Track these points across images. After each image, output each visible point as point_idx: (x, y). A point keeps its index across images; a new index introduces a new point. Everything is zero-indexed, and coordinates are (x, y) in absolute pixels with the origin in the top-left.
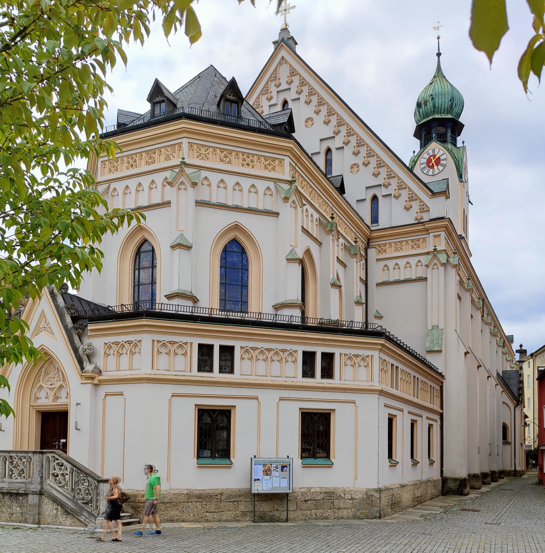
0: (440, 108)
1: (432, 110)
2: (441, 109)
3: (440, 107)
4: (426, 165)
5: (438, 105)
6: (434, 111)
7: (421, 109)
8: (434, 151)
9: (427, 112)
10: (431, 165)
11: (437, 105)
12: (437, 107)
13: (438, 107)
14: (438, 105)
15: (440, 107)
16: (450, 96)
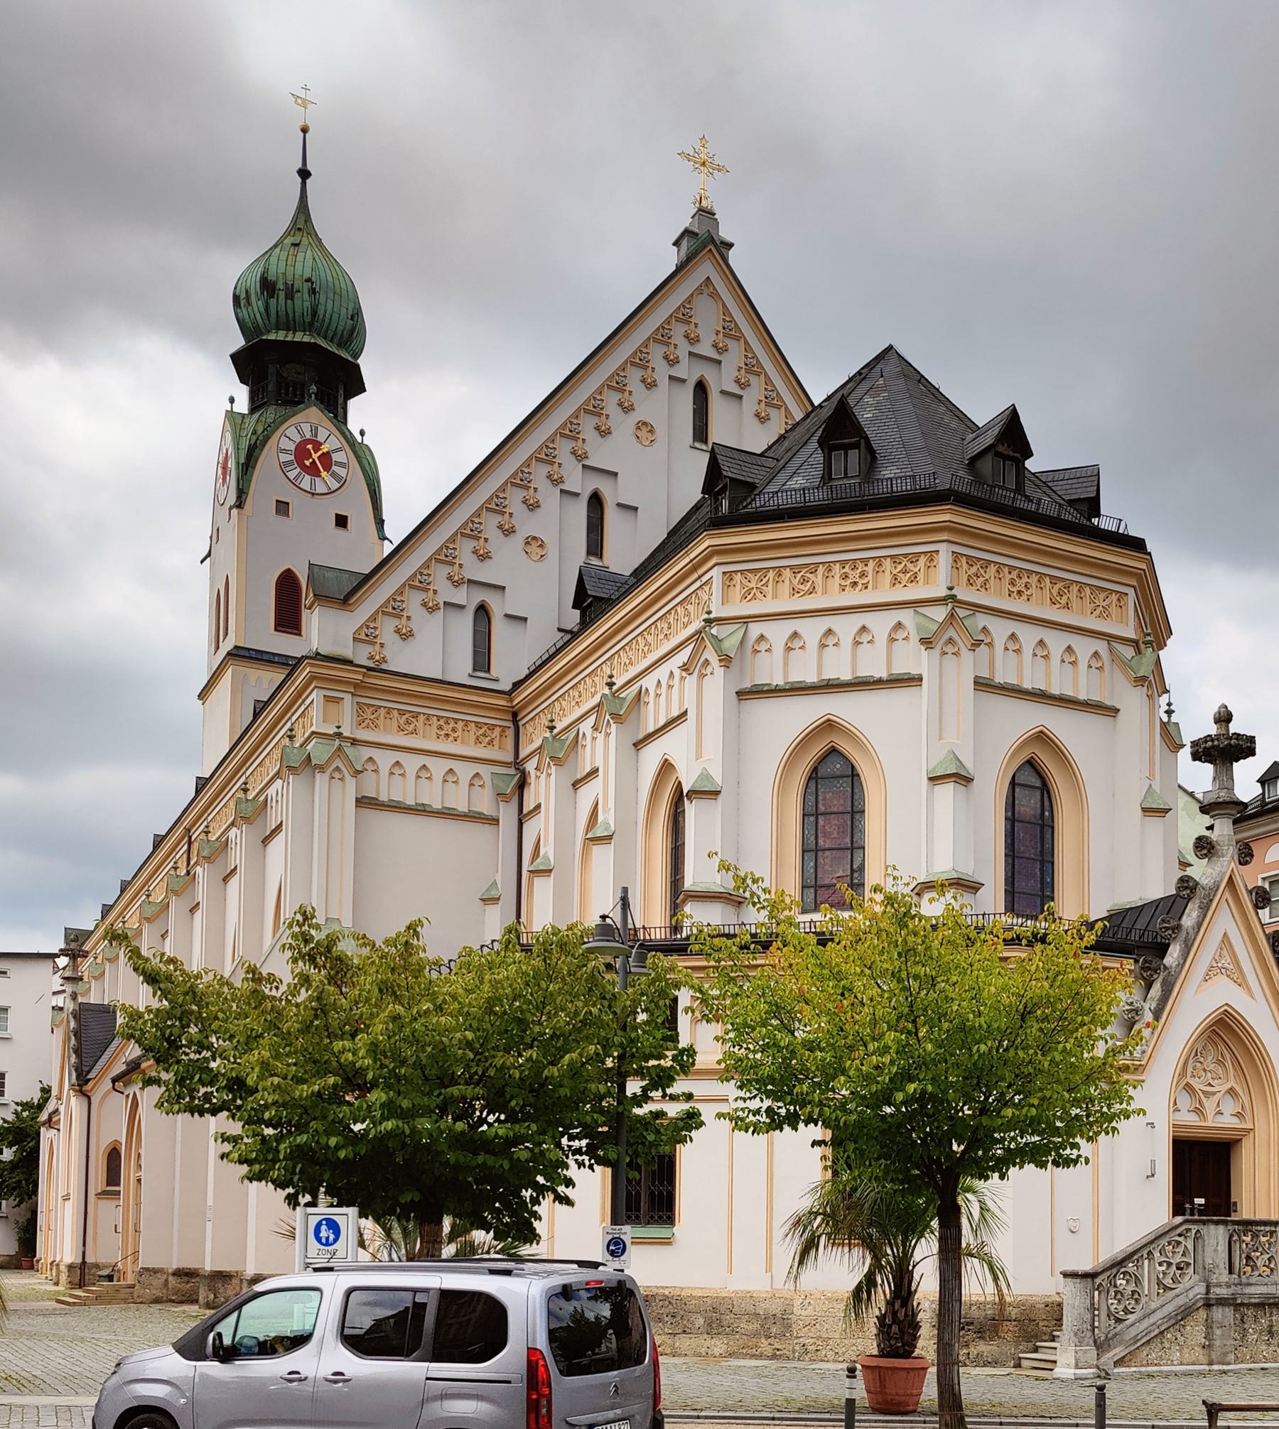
0: (326, 325)
1: (308, 319)
2: (328, 329)
3: (326, 325)
4: (292, 457)
5: (324, 316)
6: (311, 324)
7: (273, 302)
8: (315, 431)
9: (291, 318)
10: (307, 463)
11: (321, 312)
12: (321, 317)
13: (323, 320)
14: (324, 316)
15: (327, 320)
16: (351, 306)
